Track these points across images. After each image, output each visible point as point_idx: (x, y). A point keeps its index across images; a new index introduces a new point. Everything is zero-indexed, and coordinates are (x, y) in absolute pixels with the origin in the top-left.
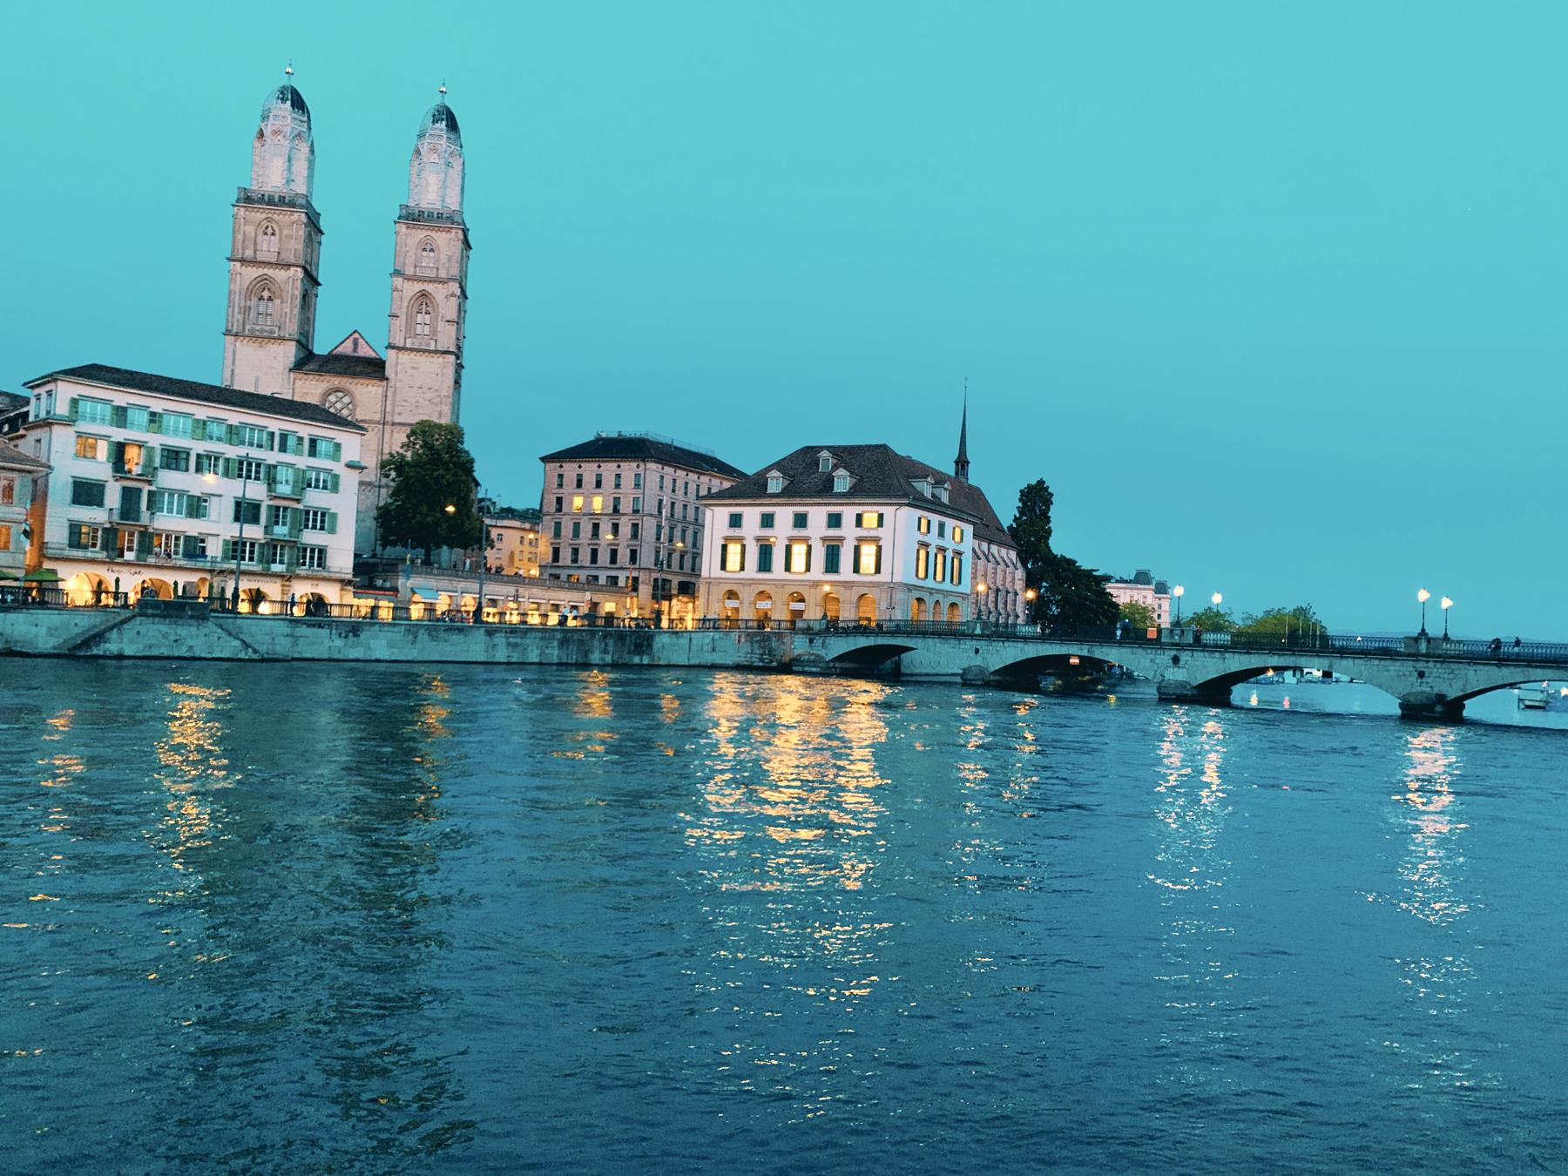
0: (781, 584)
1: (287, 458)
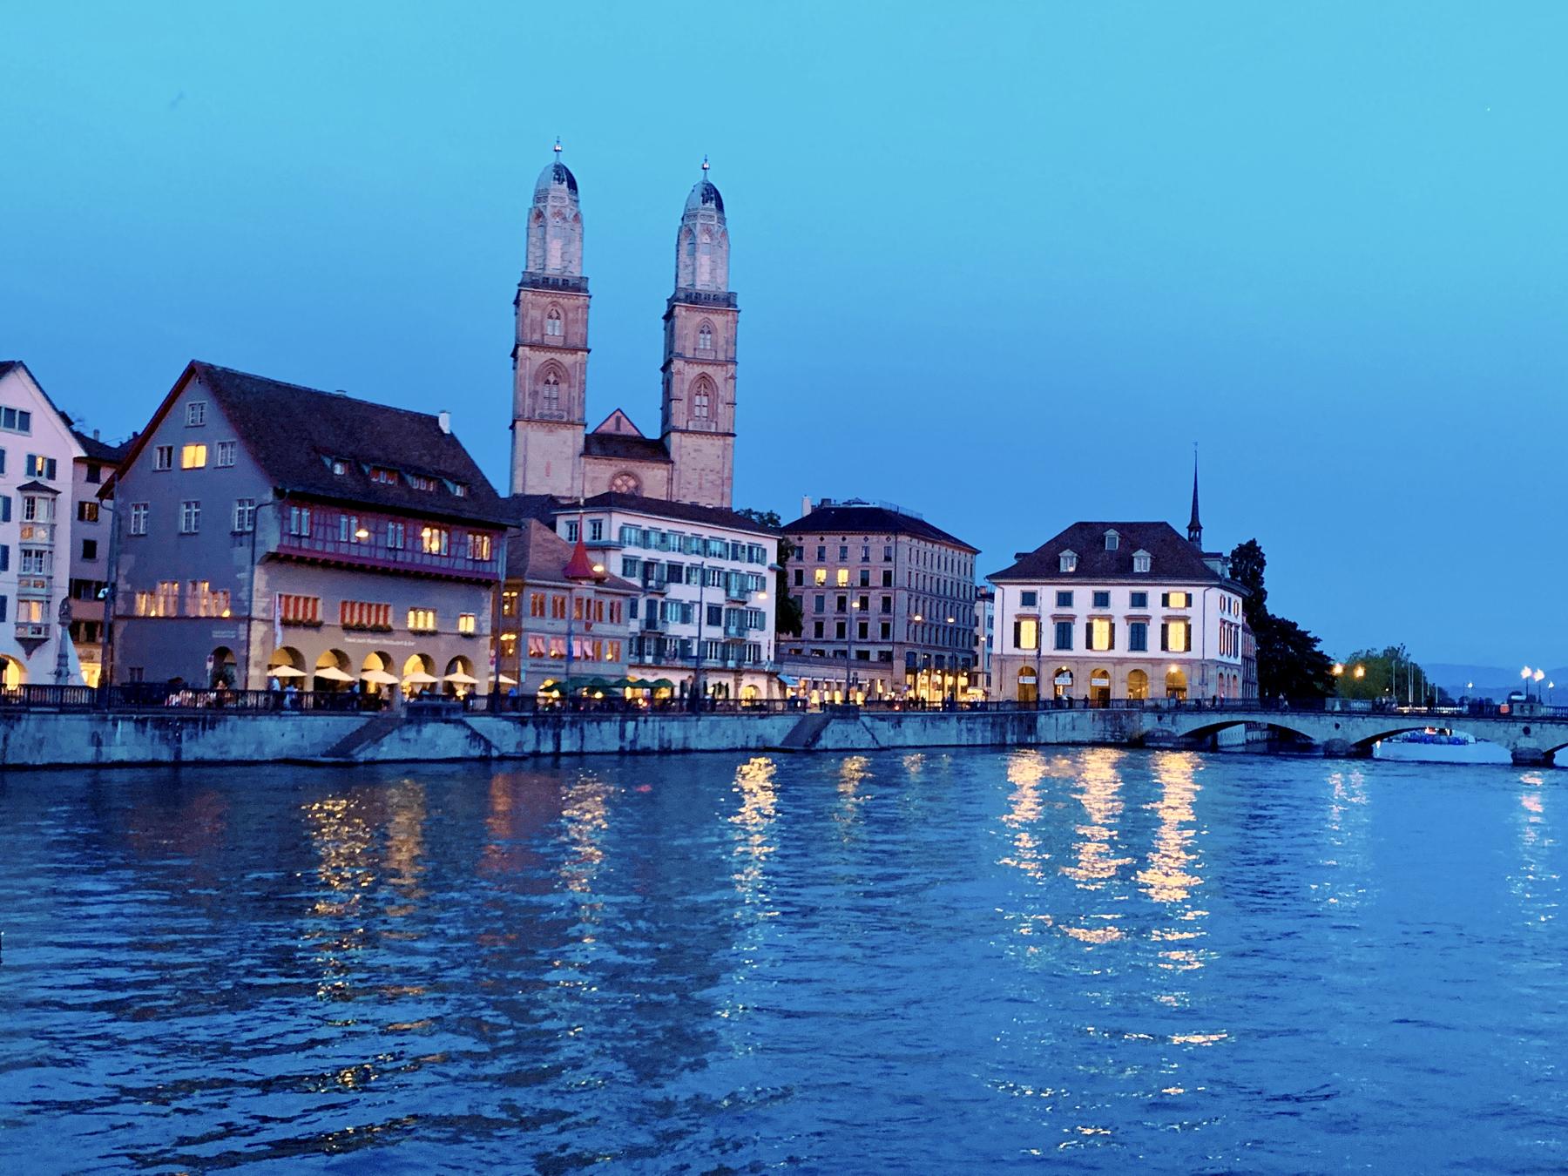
0: (1078, 660)
1: (736, 565)
